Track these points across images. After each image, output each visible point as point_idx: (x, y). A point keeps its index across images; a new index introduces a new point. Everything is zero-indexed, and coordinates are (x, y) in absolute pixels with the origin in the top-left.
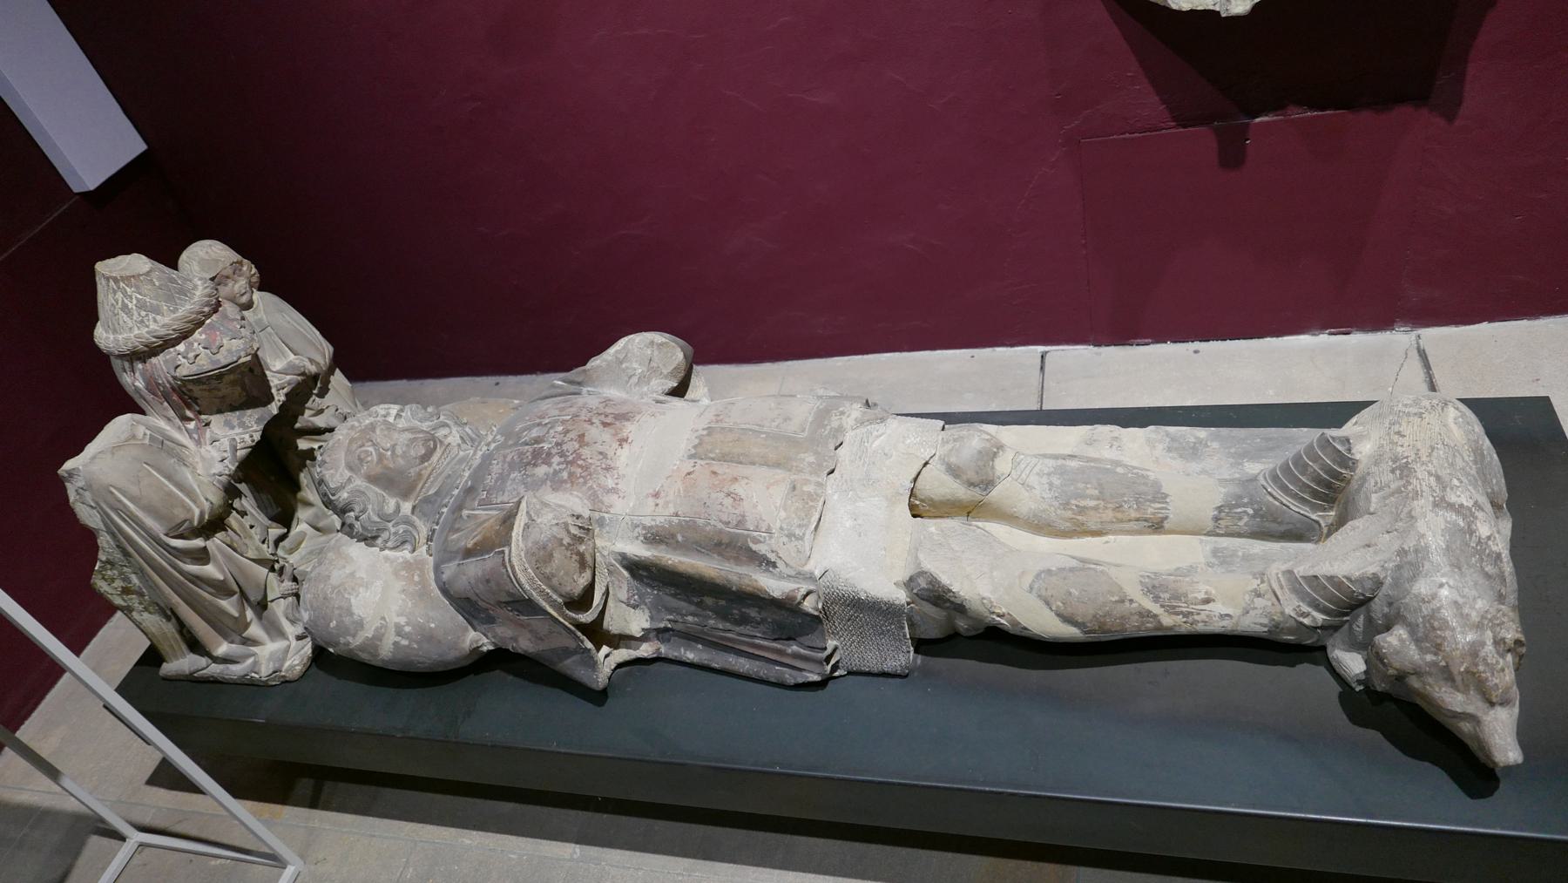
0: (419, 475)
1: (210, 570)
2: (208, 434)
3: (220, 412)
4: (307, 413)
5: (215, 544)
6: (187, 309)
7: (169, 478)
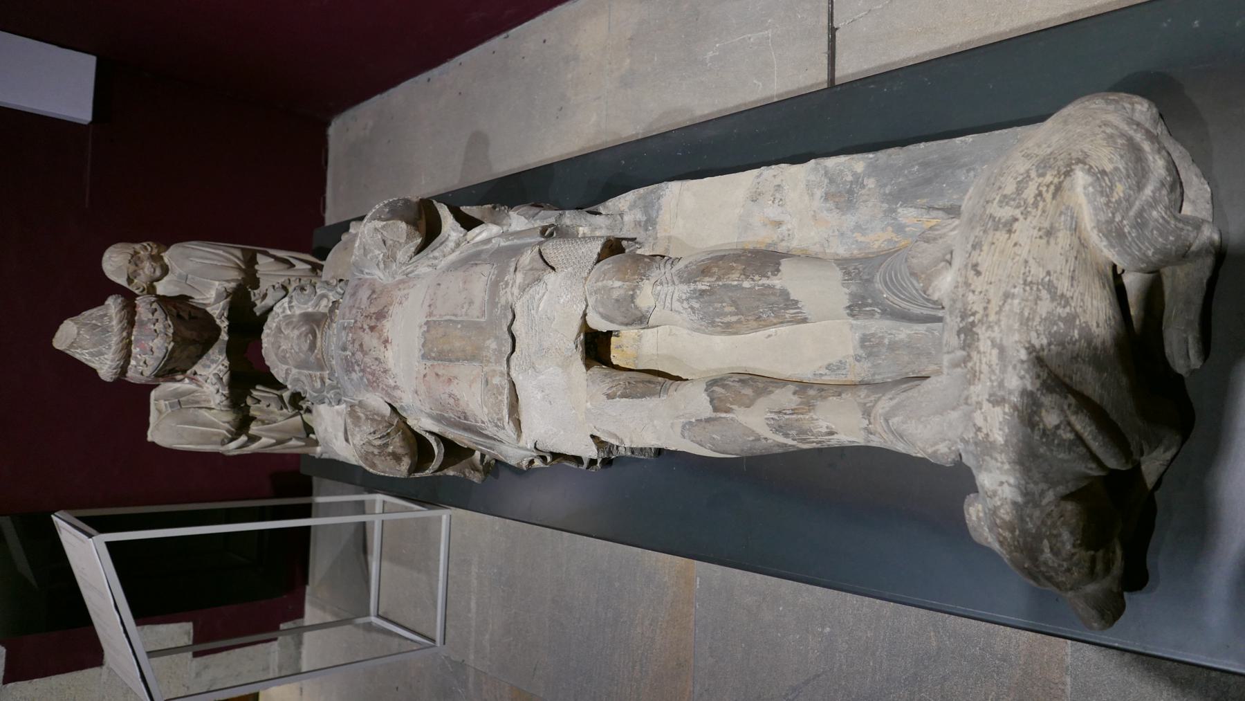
0: (318, 360)
3: (194, 363)
4: (258, 302)
5: (254, 429)
6: (115, 340)
7: (195, 423)
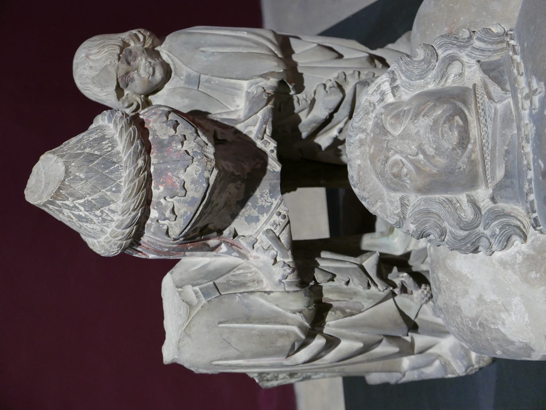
0: (472, 163)
1: (346, 346)
2: (242, 242)
3: (234, 216)
4: (302, 115)
5: (331, 324)
6: (125, 176)
7: (248, 319)
